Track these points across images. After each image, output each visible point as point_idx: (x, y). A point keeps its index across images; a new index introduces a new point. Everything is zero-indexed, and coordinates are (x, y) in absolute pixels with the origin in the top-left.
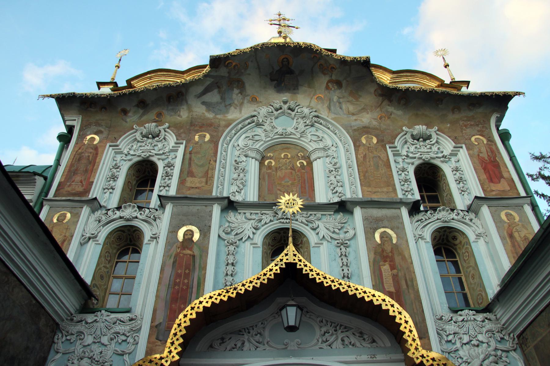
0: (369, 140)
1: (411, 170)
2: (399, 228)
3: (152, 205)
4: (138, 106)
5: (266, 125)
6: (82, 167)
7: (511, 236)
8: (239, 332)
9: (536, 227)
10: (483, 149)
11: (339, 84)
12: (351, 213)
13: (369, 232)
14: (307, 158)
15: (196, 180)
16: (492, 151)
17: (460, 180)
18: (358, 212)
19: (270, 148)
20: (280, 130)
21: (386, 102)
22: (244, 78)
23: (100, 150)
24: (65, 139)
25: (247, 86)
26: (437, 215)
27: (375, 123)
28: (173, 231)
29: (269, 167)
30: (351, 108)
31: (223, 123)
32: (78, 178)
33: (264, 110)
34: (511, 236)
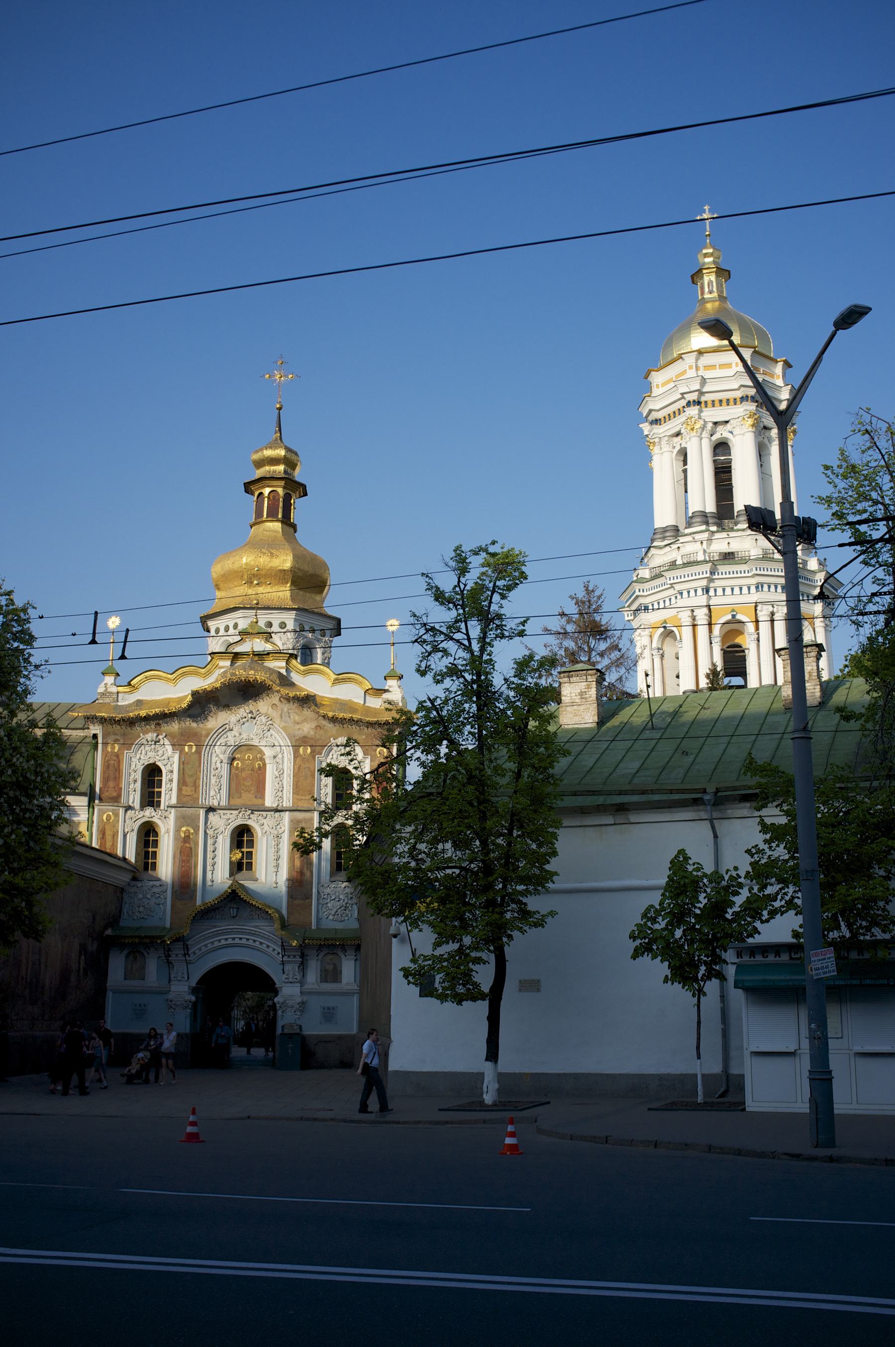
0: (305, 751)
3: (162, 807)
5: (235, 729)
14: (262, 759)
15: (189, 789)
23: (121, 757)
27: (312, 733)
28: (177, 830)
30: (297, 718)
31: (204, 732)
32: (111, 784)
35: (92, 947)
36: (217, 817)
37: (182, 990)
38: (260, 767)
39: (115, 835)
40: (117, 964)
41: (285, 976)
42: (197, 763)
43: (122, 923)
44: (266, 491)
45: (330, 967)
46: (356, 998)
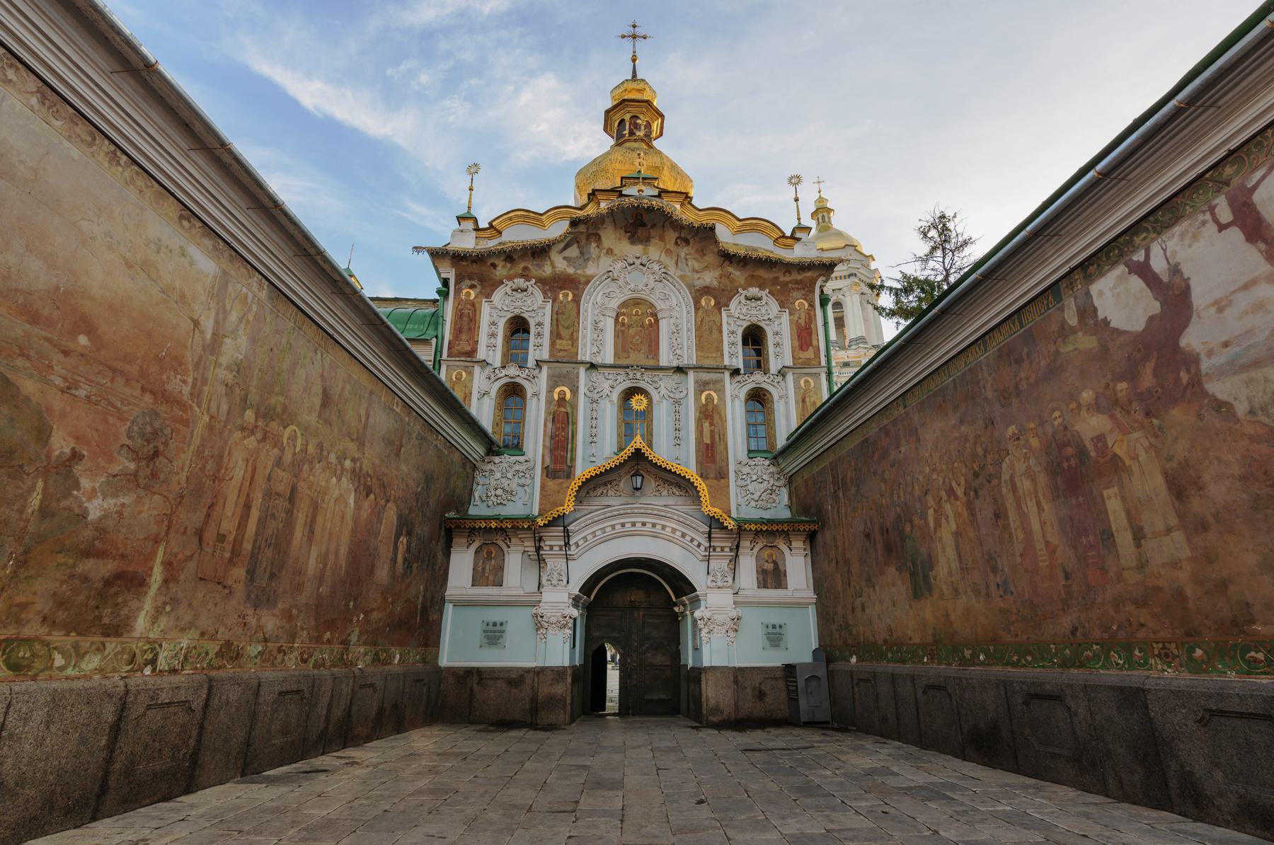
1: (740, 332)
2: (721, 392)
4: (505, 260)
6: (465, 327)
7: (804, 401)
8: (605, 484)
9: (826, 396)
10: (803, 315)
11: (687, 242)
12: (686, 374)
13: (699, 392)
14: (655, 315)
15: (564, 342)
16: (810, 318)
17: (777, 345)
18: (691, 374)
19: (624, 304)
20: (632, 286)
21: (727, 263)
22: (601, 233)
24: (444, 293)
25: (603, 239)
26: (753, 378)
27: (715, 283)
29: (623, 324)
30: (696, 265)
32: (464, 337)
33: (619, 265)
34: (804, 401)
35: (423, 530)
36: (601, 377)
37: (560, 600)
38: (651, 324)
39: (468, 396)
40: (462, 563)
41: (710, 578)
42: (575, 313)
43: (472, 511)
44: (627, 117)
45: (770, 566)
46: (811, 612)
